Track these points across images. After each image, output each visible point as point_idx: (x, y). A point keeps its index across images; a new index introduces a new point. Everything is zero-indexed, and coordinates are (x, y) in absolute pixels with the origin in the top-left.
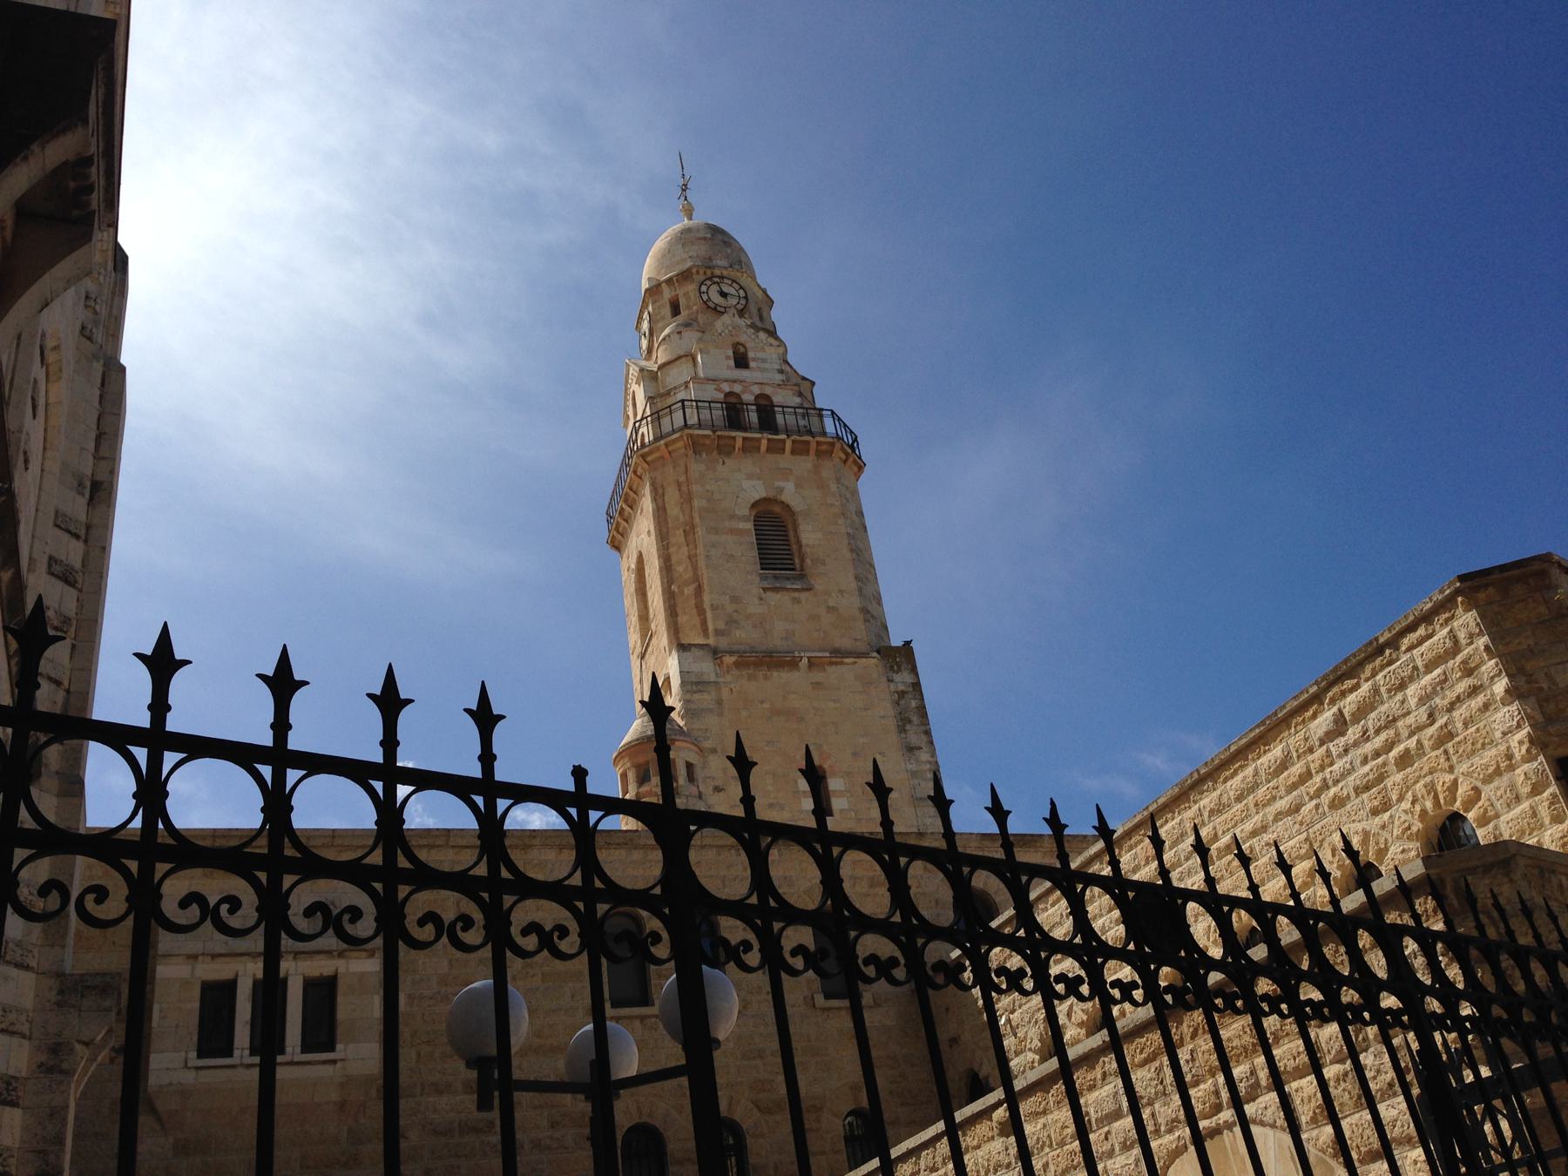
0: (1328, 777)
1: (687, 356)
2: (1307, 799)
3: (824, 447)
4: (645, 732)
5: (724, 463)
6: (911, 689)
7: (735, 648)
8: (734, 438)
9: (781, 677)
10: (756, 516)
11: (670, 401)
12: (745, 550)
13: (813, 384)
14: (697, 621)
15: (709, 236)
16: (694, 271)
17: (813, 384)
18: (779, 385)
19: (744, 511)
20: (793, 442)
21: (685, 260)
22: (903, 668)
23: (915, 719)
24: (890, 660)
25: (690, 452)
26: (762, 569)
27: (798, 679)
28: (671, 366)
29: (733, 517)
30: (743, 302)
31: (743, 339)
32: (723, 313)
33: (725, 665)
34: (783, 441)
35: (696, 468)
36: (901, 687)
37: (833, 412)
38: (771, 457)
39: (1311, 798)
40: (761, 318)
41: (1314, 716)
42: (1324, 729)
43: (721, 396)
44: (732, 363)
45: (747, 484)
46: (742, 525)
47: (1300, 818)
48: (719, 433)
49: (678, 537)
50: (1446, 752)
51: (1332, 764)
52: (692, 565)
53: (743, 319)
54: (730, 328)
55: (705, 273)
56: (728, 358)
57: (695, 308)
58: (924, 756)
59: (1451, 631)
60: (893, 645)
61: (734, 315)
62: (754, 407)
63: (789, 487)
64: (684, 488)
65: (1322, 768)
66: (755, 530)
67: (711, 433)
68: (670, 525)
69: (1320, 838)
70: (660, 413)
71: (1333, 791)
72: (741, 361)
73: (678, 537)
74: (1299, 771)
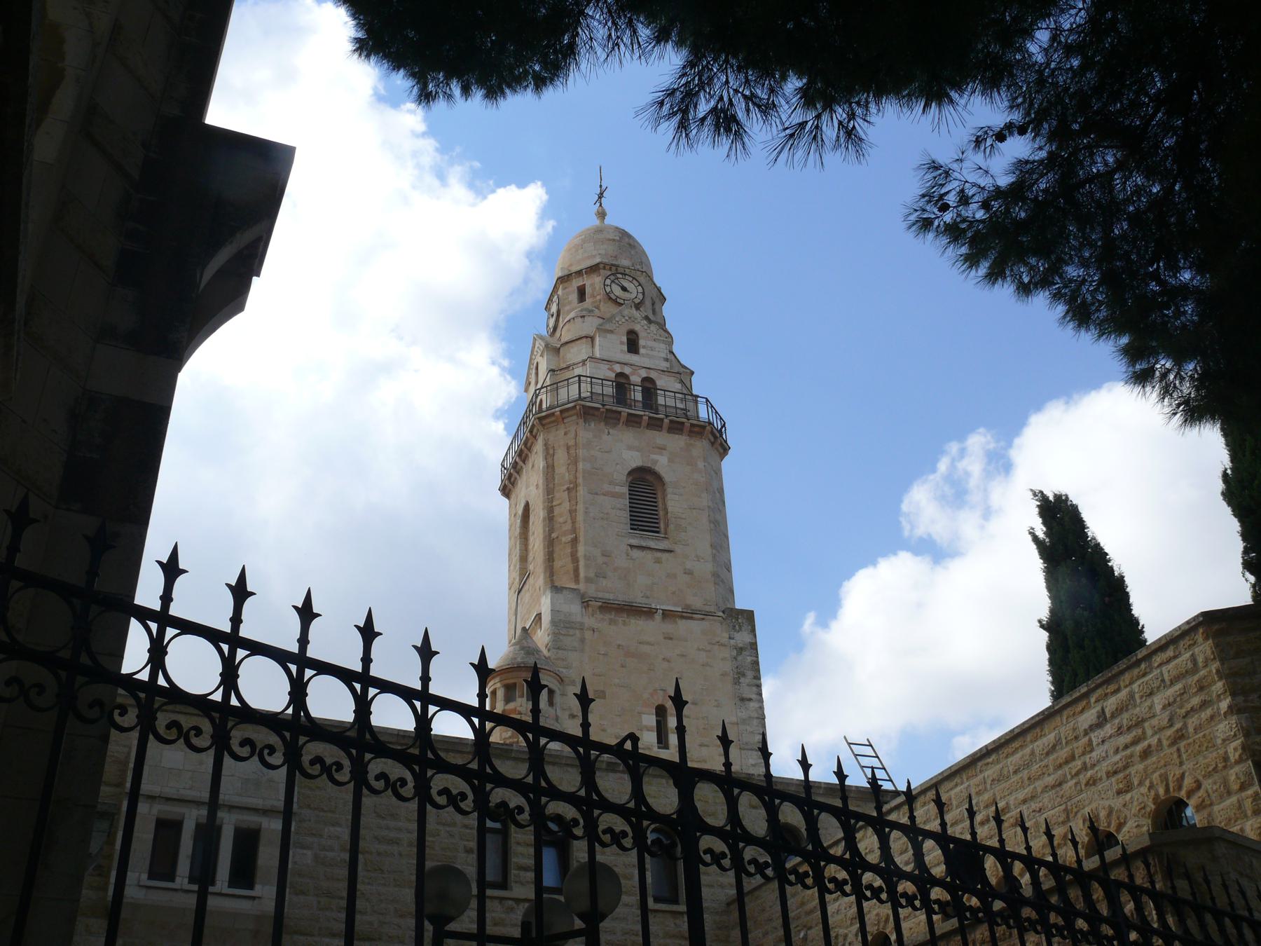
0: (1087, 762)
1: (587, 337)
2: (1069, 777)
3: (696, 429)
4: (515, 658)
5: (609, 433)
7: (600, 595)
8: (620, 412)
9: (638, 625)
10: (631, 483)
11: (568, 374)
12: (618, 508)
13: (692, 373)
14: (570, 567)
15: (618, 238)
16: (601, 266)
17: (692, 373)
19: (621, 475)
20: (671, 421)
21: (594, 256)
22: (743, 630)
23: (750, 674)
24: (734, 620)
26: (632, 529)
27: (651, 629)
28: (573, 344)
29: (611, 483)
30: (640, 296)
31: (637, 328)
32: (622, 304)
34: (662, 420)
37: (707, 400)
38: (651, 434)
39: (1072, 777)
40: (654, 312)
41: (1082, 711)
42: (1089, 723)
43: (613, 375)
44: (625, 348)
46: (618, 489)
47: (1062, 792)
48: (608, 407)
49: (561, 495)
50: (1178, 750)
51: (1092, 750)
52: (571, 519)
53: (639, 311)
56: (622, 343)
57: (598, 297)
58: (753, 705)
59: (1192, 655)
60: (737, 607)
62: (640, 388)
64: (572, 451)
65: (1084, 754)
66: (629, 494)
67: (600, 406)
68: (556, 481)
69: (1075, 810)
70: (559, 384)
71: (1089, 773)
72: (633, 345)
73: (561, 495)
74: (1066, 755)
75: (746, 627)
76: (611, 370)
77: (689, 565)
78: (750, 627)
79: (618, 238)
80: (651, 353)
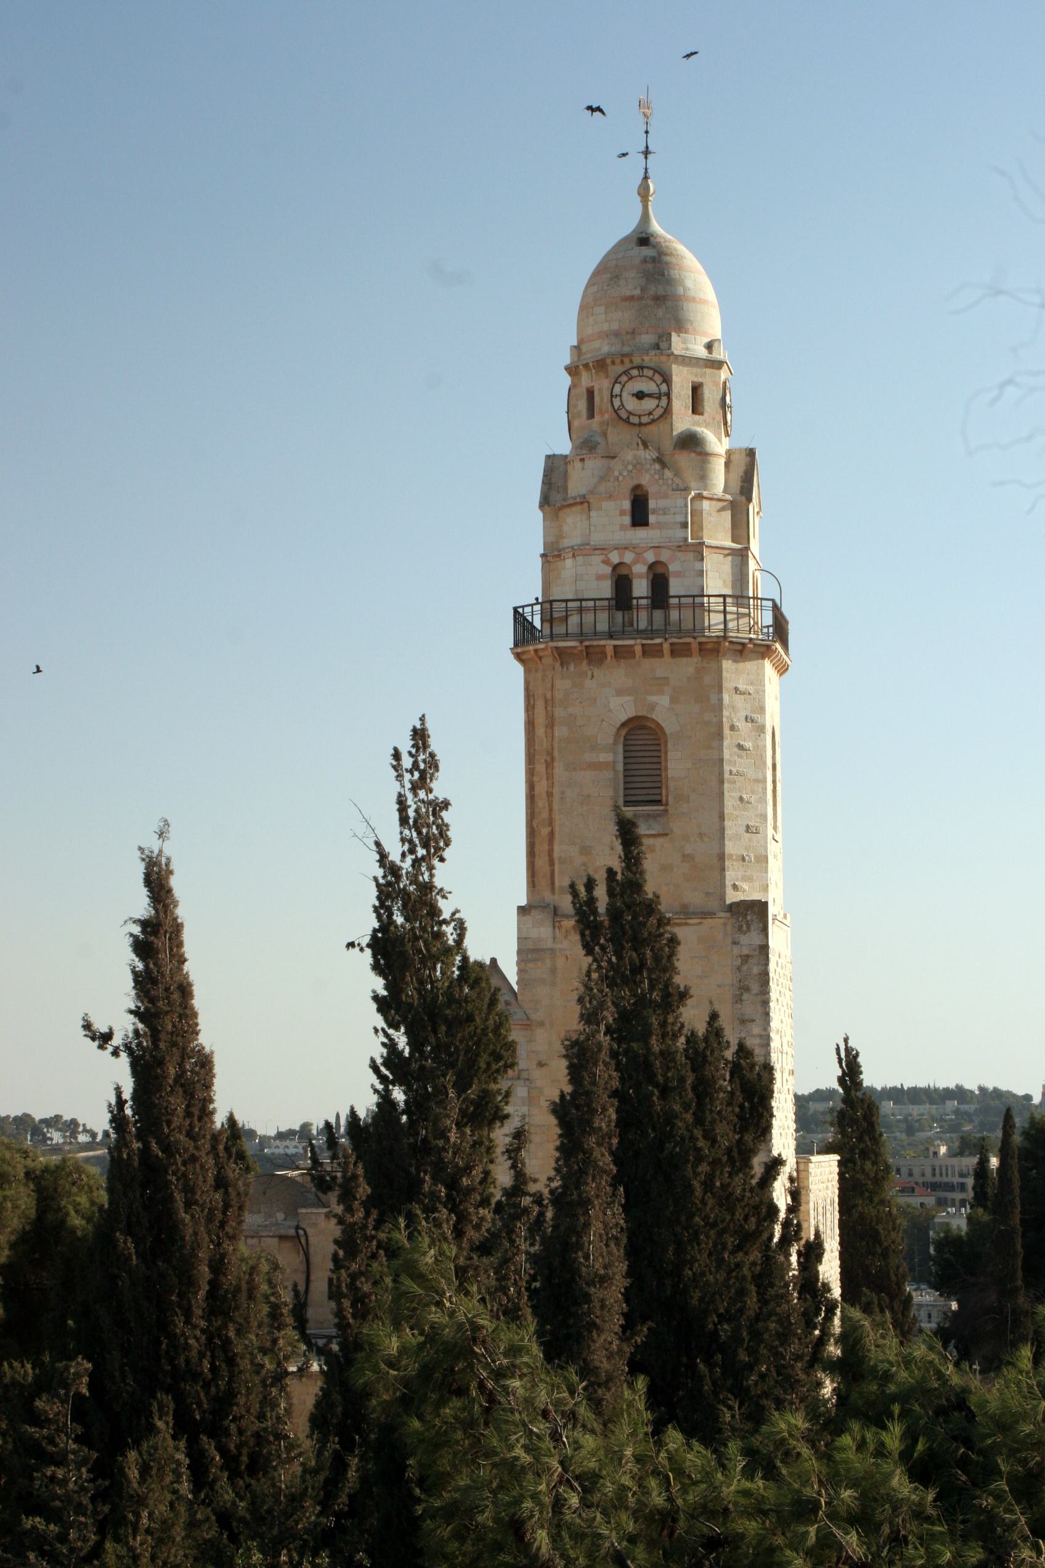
6: (757, 953)
18: (679, 546)
20: (671, 644)
23: (755, 987)
25: (558, 665)
31: (645, 480)
33: (563, 930)
34: (661, 644)
35: (563, 685)
36: (745, 951)
38: (648, 663)
44: (627, 520)
45: (615, 702)
48: (587, 643)
49: (541, 768)
54: (630, 467)
55: (622, 362)
56: (622, 513)
61: (638, 445)
63: (664, 701)
72: (639, 515)
75: (756, 926)
76: (606, 562)
77: (688, 850)
78: (761, 925)
79: (637, 292)
80: (662, 518)
